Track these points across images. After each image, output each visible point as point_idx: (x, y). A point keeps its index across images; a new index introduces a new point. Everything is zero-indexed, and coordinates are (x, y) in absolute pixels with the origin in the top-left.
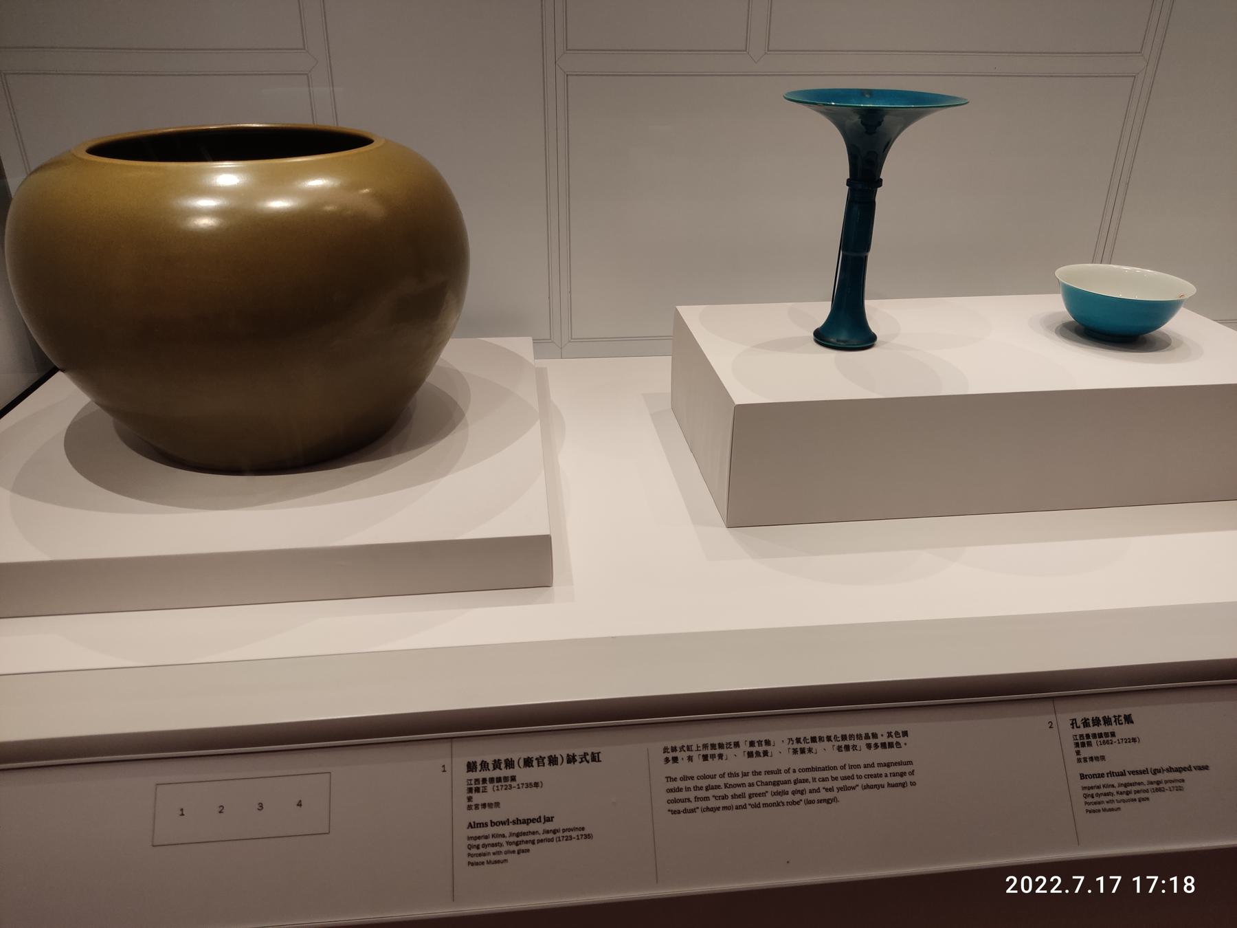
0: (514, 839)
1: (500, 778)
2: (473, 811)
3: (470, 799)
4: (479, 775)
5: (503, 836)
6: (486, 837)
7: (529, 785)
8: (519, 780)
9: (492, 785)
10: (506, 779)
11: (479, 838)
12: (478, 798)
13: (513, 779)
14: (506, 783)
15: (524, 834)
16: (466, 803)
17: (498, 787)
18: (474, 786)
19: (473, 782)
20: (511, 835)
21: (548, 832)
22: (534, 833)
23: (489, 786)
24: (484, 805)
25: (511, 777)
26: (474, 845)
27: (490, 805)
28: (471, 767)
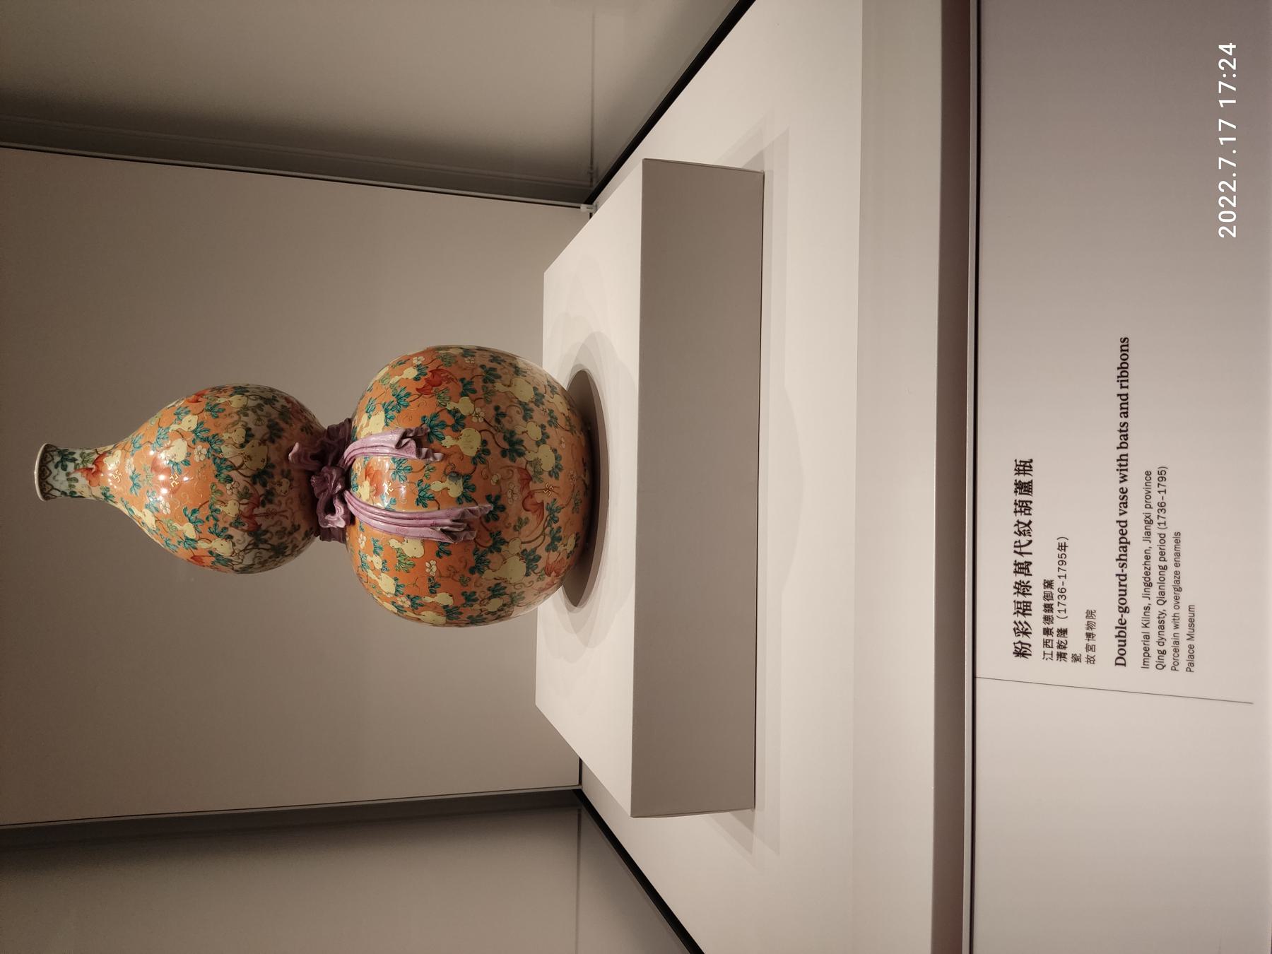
0: (1154, 591)
1: (1045, 606)
2: (1098, 654)
3: (1076, 658)
4: (1036, 639)
5: (1147, 608)
6: (1147, 637)
7: (1062, 562)
8: (1052, 575)
9: (1056, 620)
10: (1048, 596)
11: (1146, 649)
12: (1076, 643)
13: (1049, 584)
14: (1055, 597)
15: (1147, 574)
16: (1083, 664)
17: (1059, 611)
18: (1056, 650)
19: (1048, 651)
20: (1146, 595)
21: (1148, 533)
22: (1147, 558)
23: (1057, 625)
24: (1089, 635)
25: (1045, 587)
26: (1155, 658)
27: (1090, 626)
28: (1021, 653)
